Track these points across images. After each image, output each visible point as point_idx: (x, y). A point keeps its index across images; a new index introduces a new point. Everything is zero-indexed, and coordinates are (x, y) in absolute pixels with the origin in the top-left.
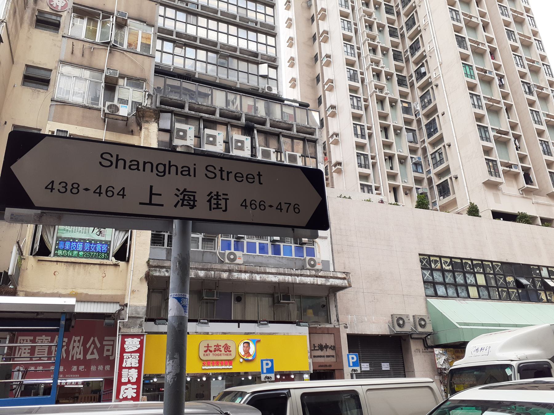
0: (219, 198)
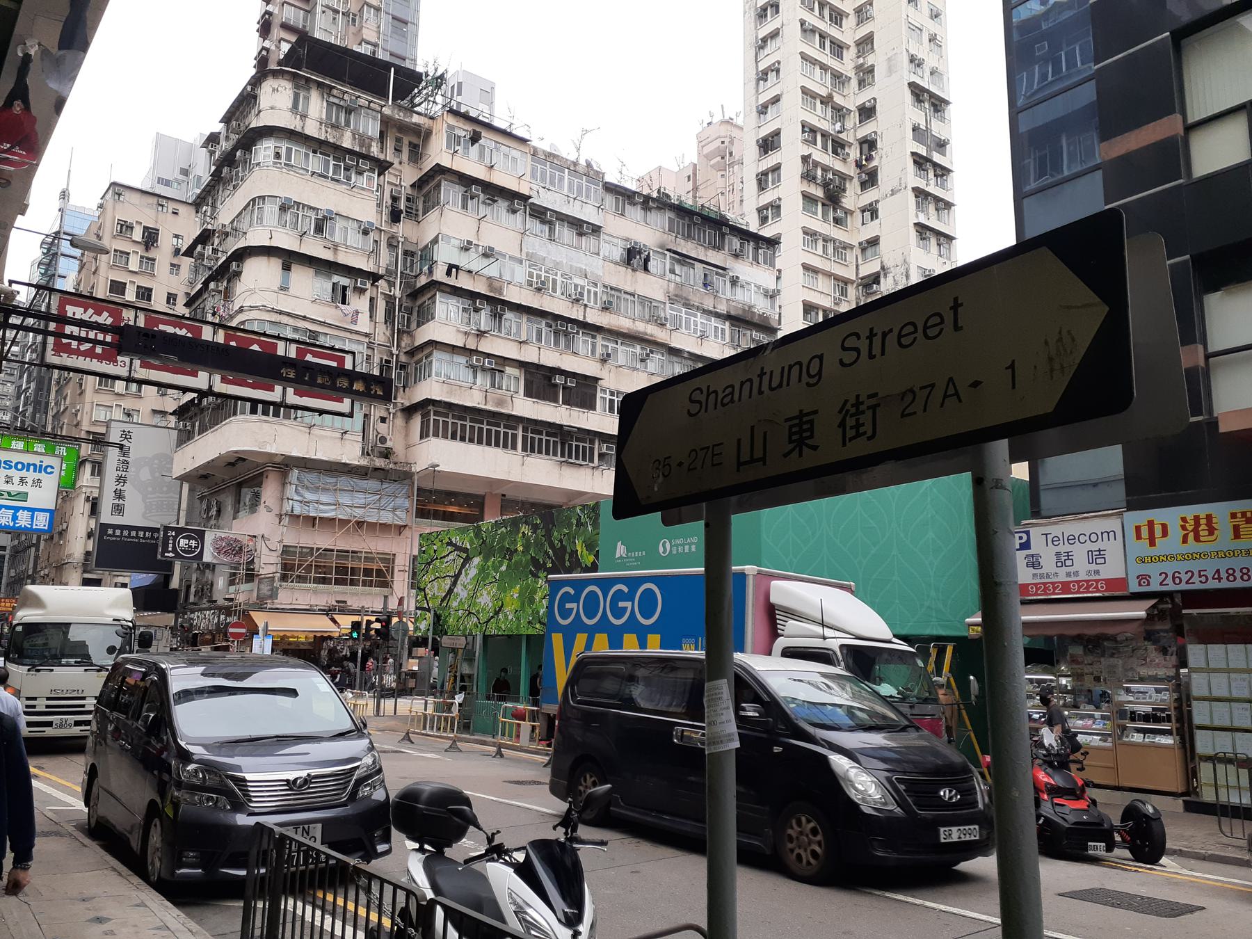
0: (862, 408)
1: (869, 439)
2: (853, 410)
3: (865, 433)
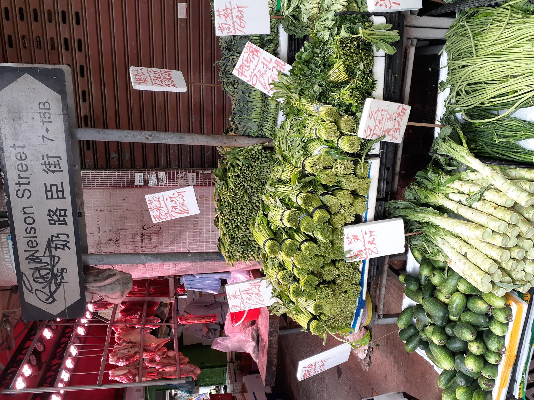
1: (61, 159)
3: (58, 161)
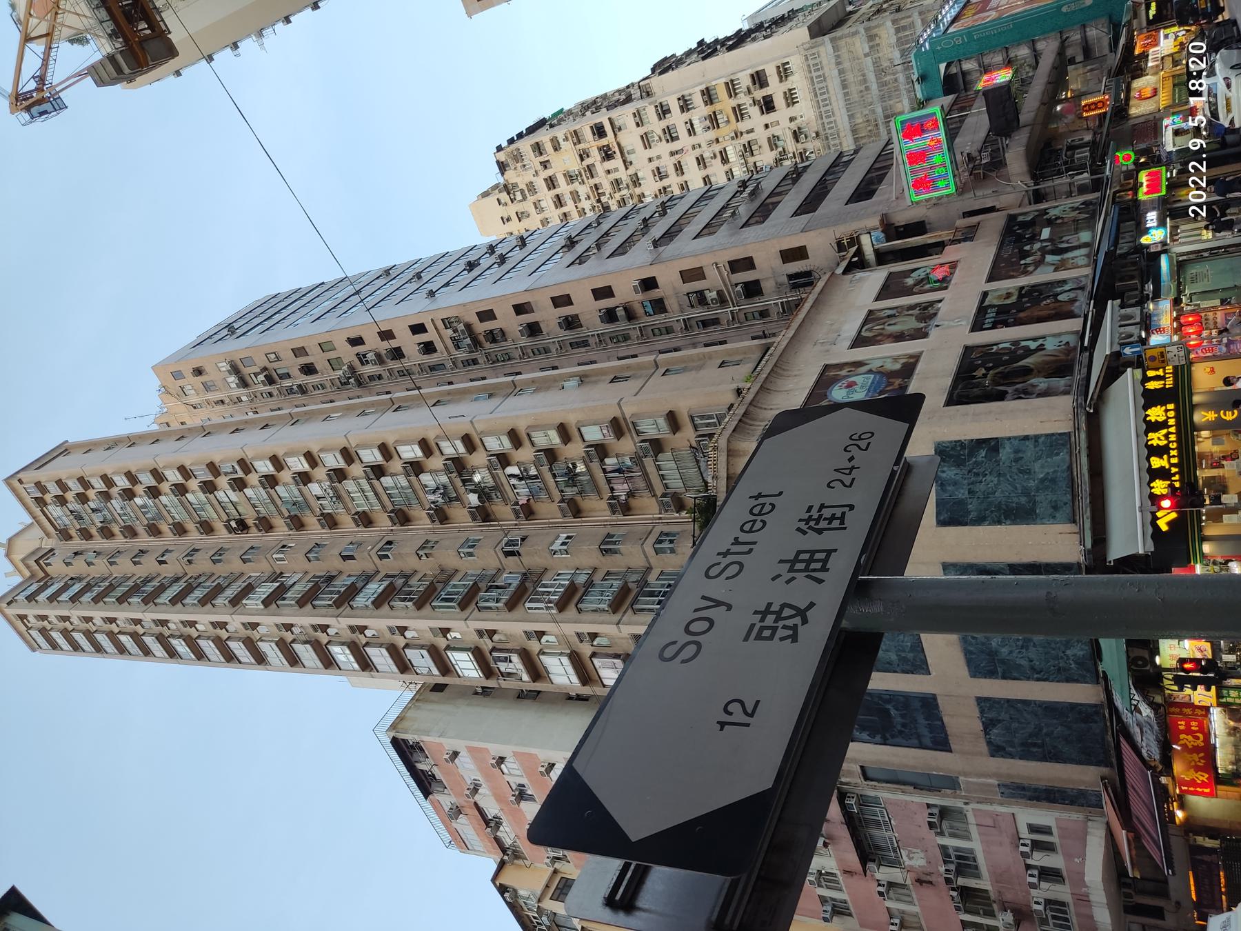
2: (812, 523)
3: (844, 514)
